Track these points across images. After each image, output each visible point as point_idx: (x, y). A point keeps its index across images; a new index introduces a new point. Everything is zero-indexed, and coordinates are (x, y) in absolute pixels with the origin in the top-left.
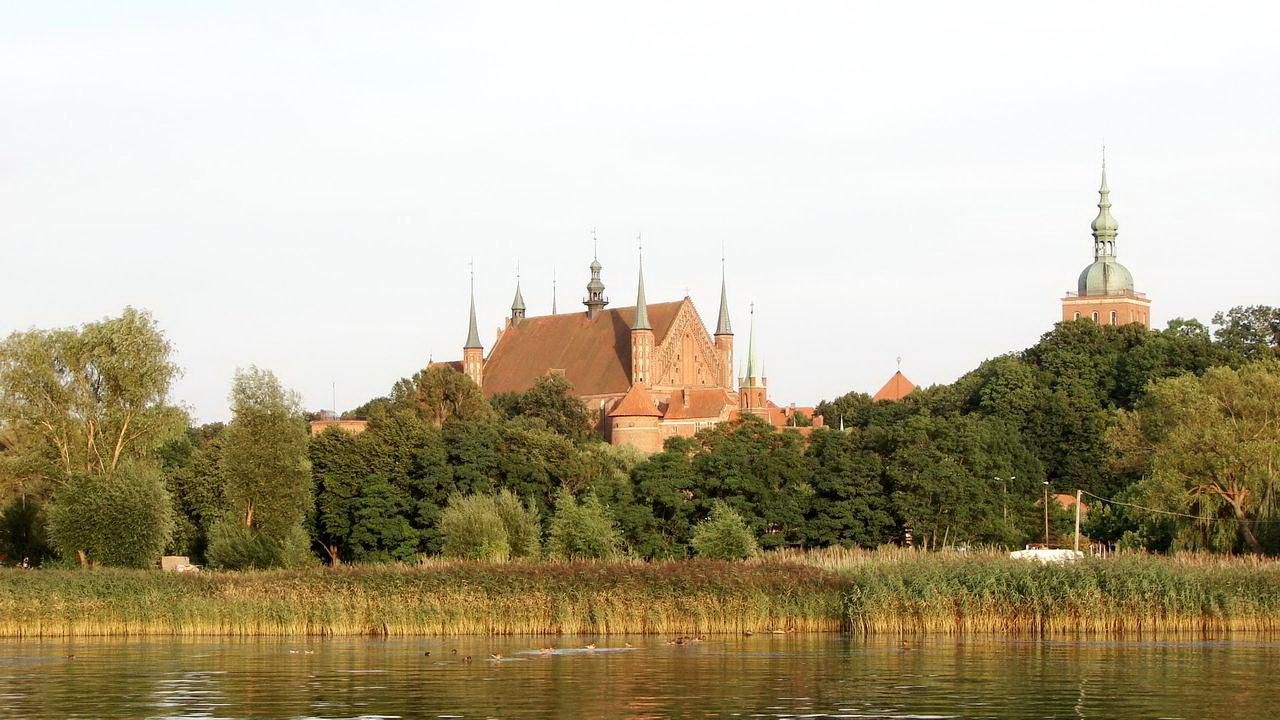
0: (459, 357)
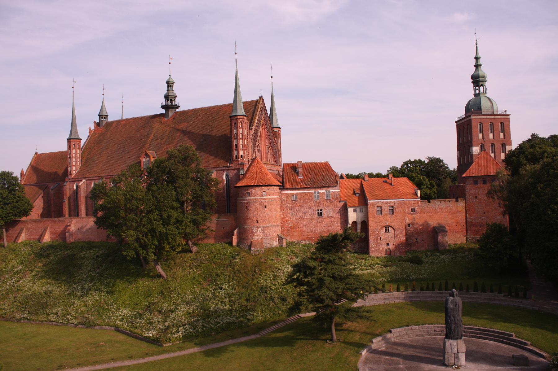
0: (64, 147)
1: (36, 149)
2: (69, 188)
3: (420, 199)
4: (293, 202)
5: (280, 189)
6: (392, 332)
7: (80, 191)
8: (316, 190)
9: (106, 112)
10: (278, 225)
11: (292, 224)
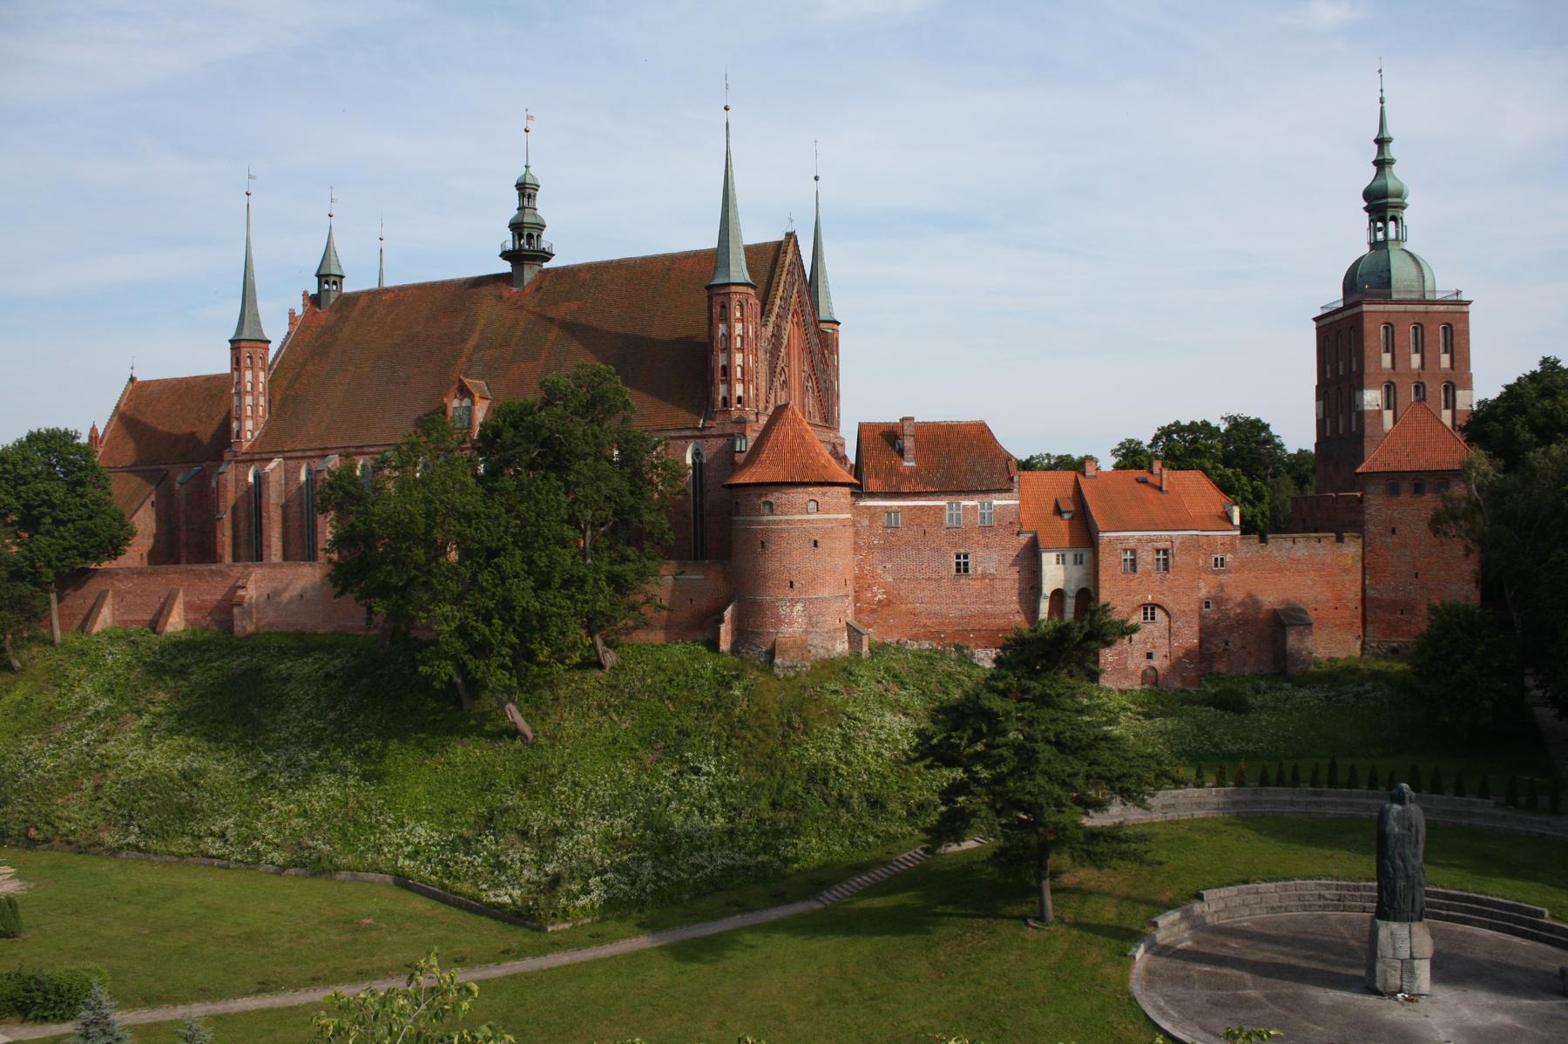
0: (219, 363)
1: (132, 368)
2: (234, 479)
3: (1238, 533)
4: (889, 531)
5: (852, 494)
6: (1205, 898)
7: (268, 488)
8: (952, 499)
9: (340, 266)
10: (847, 596)
11: (884, 593)
